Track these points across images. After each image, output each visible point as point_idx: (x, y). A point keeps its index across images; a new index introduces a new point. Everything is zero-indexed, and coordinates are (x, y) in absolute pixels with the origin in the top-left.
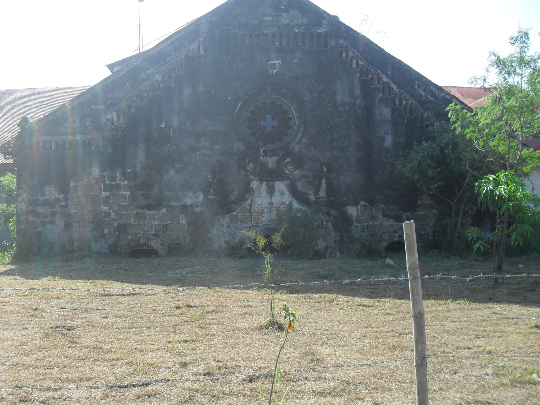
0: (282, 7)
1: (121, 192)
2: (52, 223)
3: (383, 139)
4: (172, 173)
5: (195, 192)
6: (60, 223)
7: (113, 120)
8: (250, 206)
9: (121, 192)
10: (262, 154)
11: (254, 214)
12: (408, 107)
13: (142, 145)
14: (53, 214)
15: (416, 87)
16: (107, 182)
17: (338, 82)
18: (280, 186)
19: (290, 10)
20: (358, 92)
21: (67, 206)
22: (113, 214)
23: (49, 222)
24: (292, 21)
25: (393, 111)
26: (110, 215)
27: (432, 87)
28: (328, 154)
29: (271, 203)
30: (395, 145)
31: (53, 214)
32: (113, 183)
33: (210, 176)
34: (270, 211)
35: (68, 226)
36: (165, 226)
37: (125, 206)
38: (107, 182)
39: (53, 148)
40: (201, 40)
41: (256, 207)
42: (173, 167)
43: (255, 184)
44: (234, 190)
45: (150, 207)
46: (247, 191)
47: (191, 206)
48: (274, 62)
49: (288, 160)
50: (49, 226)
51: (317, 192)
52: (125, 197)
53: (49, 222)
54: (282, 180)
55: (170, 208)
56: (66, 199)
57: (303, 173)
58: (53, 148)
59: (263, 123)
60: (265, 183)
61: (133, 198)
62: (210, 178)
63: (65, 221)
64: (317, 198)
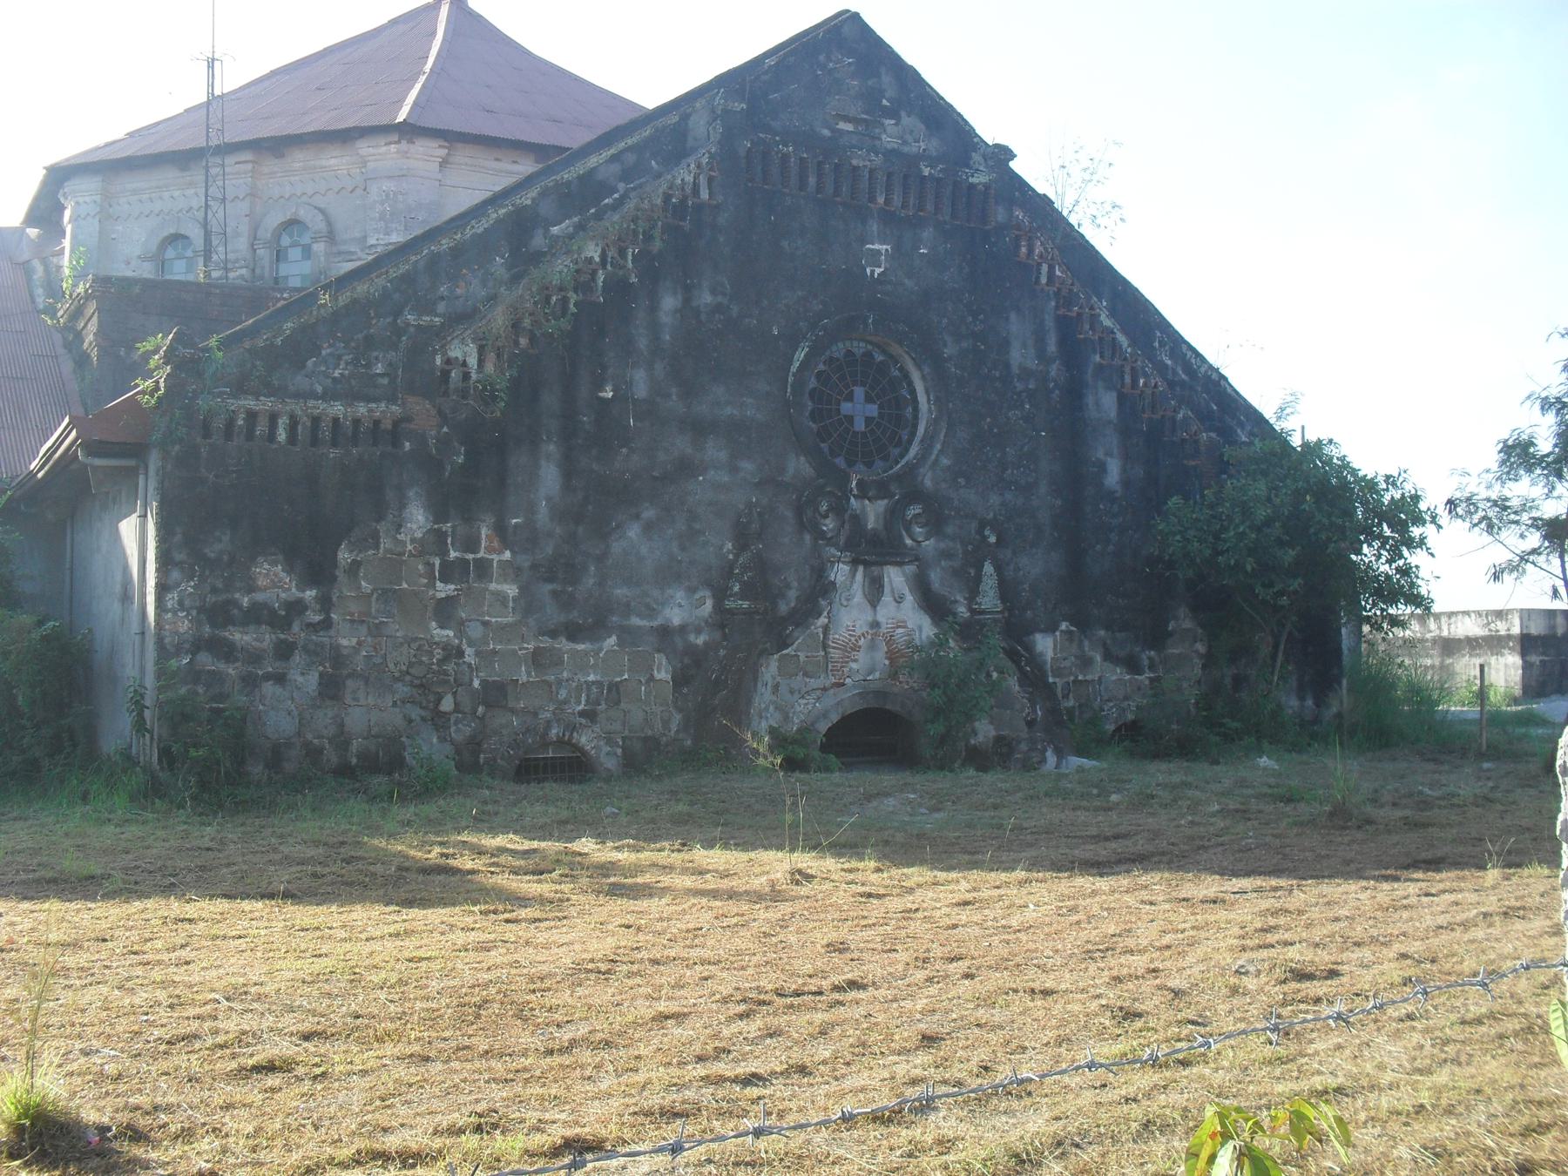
0: (885, 102)
1: (493, 586)
2: (280, 679)
3: (1102, 468)
4: (634, 531)
5: (692, 590)
6: (307, 680)
7: (464, 364)
8: (826, 629)
9: (493, 586)
10: (855, 492)
11: (835, 654)
12: (1149, 391)
13: (552, 447)
14: (284, 651)
15: (1156, 344)
16: (453, 554)
17: (1013, 316)
18: (896, 578)
19: (903, 114)
20: (1052, 347)
21: (327, 624)
22: (469, 651)
23: (267, 677)
24: (905, 142)
25: (1121, 398)
26: (461, 654)
27: (1184, 347)
28: (994, 499)
29: (875, 625)
30: (1126, 483)
31: (284, 651)
32: (470, 556)
33: (730, 546)
34: (872, 646)
35: (331, 688)
36: (614, 687)
37: (503, 627)
38: (453, 554)
39: (282, 436)
40: (705, 160)
41: (840, 635)
42: (637, 517)
43: (840, 572)
44: (788, 586)
45: (573, 632)
46: (820, 590)
47: (683, 629)
48: (876, 247)
49: (914, 510)
50: (269, 688)
51: (973, 592)
52: (502, 598)
53: (267, 677)
54: (900, 564)
55: (628, 636)
56: (325, 603)
57: (942, 545)
58: (282, 436)
59: (846, 407)
60: (861, 568)
61: (527, 604)
62: (729, 552)
63: (321, 675)
64: (973, 611)
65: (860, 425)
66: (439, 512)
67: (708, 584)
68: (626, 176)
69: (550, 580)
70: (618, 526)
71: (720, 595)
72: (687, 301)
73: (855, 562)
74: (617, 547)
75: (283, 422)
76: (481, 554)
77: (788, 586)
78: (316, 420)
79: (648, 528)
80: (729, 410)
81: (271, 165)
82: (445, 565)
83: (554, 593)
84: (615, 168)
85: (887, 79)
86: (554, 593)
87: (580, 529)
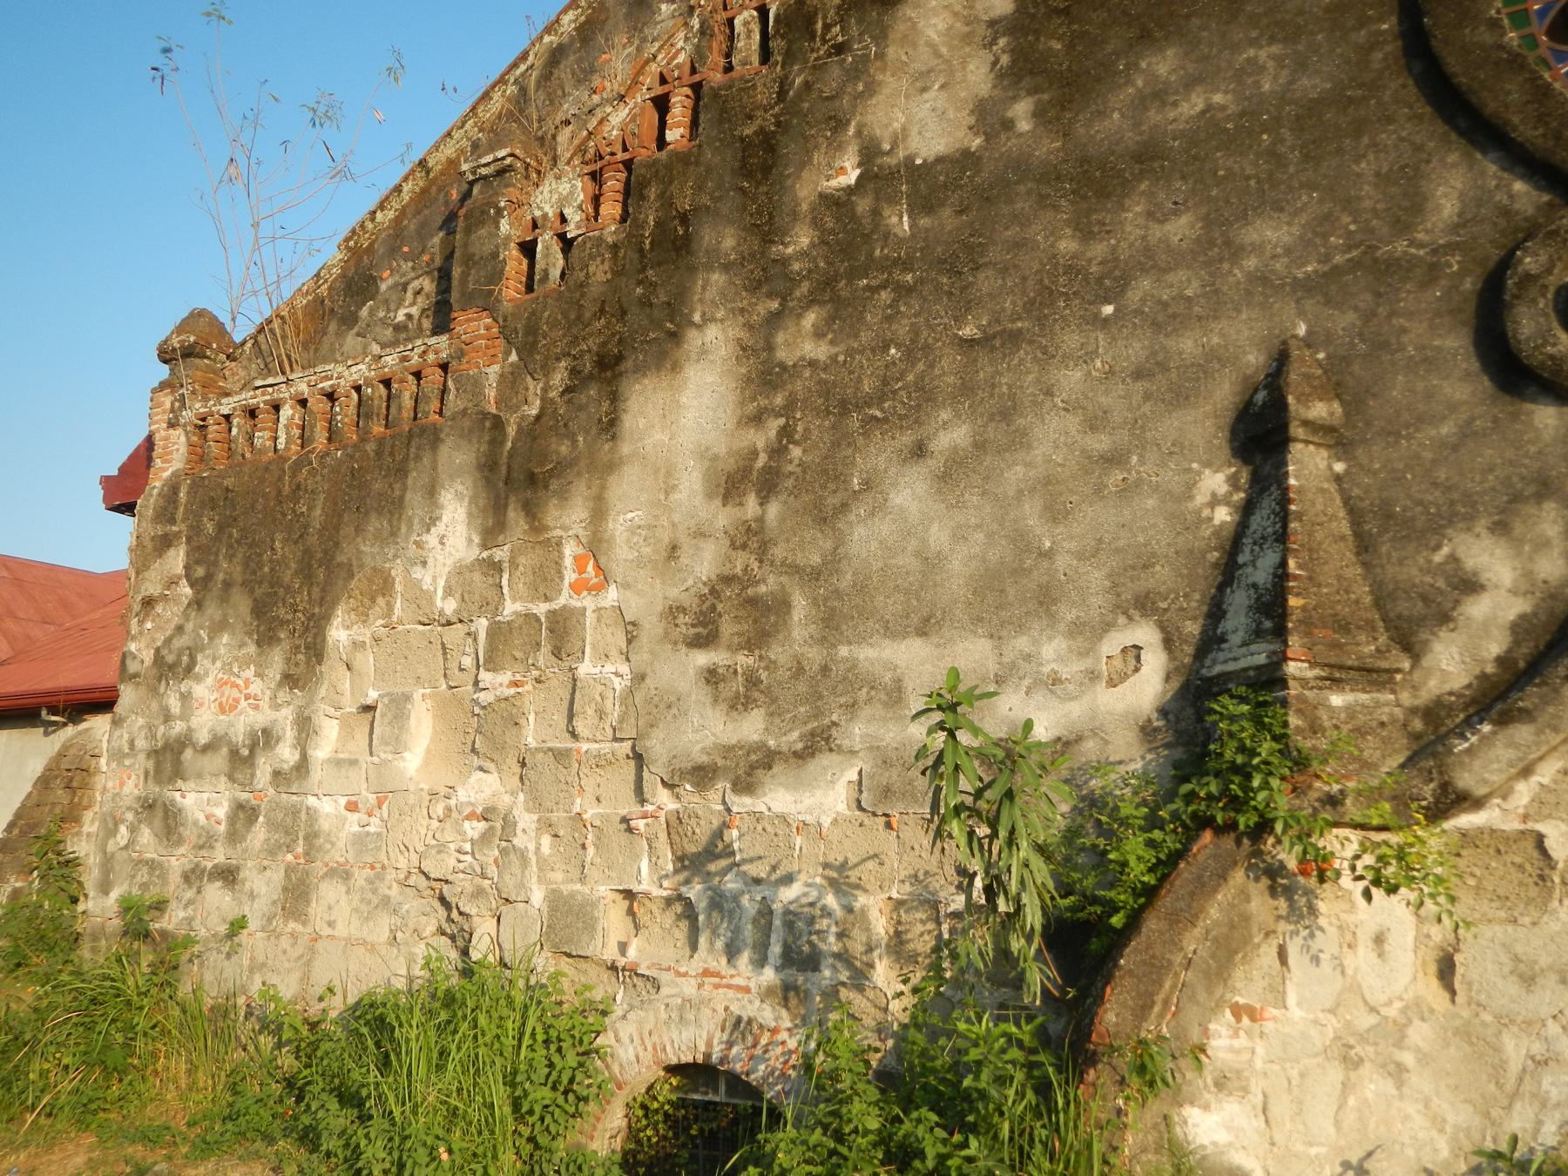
2: (228, 875)
4: (909, 493)
6: (263, 884)
13: (712, 332)
16: (511, 608)
21: (303, 766)
32: (541, 609)
33: (1215, 481)
38: (511, 608)
42: (919, 451)
44: (1470, 585)
56: (305, 727)
62: (1214, 502)
63: (289, 869)
67: (1144, 605)
69: (698, 643)
70: (867, 485)
74: (865, 537)
76: (562, 601)
77: (1470, 585)
79: (948, 477)
80: (1192, 105)
82: (496, 631)
83: (712, 676)
86: (712, 676)
87: (773, 510)
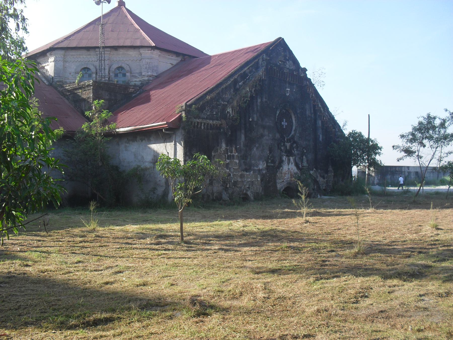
1: (235, 160)
4: (255, 149)
5: (263, 162)
9: (235, 160)
11: (283, 175)
18: (292, 159)
20: (312, 111)
22: (232, 174)
25: (322, 122)
26: (230, 175)
29: (289, 169)
30: (323, 140)
34: (288, 174)
36: (252, 182)
37: (236, 169)
41: (284, 171)
43: (284, 158)
45: (246, 170)
46: (281, 162)
49: (295, 145)
51: (302, 162)
52: (236, 163)
54: (292, 156)
55: (254, 171)
61: (240, 165)
64: (302, 166)
65: (284, 127)
66: (227, 145)
68: (250, 73)
71: (267, 163)
72: (262, 100)
73: (286, 156)
75: (203, 124)
78: (208, 124)
79: (257, 148)
80: (268, 124)
81: (114, 52)
84: (248, 71)
85: (288, 53)
